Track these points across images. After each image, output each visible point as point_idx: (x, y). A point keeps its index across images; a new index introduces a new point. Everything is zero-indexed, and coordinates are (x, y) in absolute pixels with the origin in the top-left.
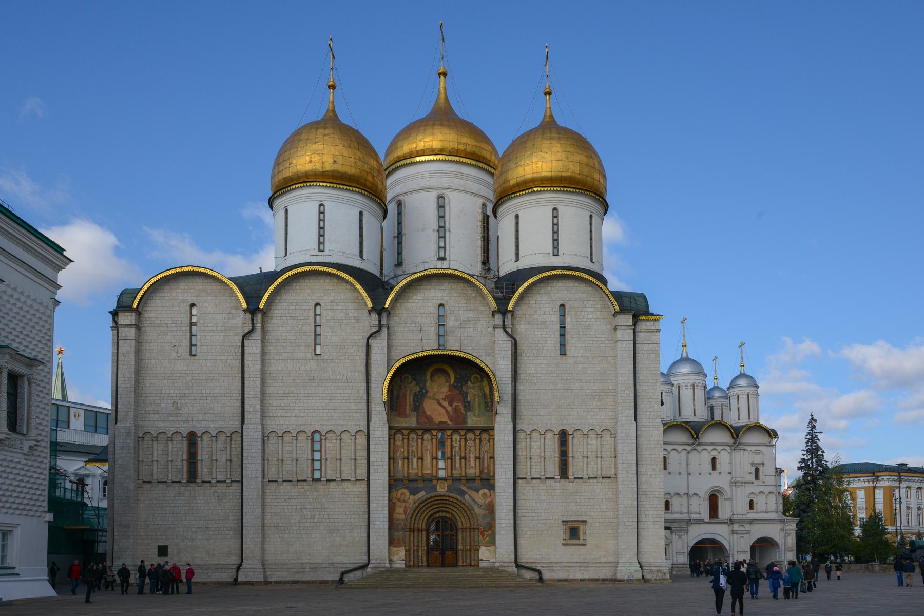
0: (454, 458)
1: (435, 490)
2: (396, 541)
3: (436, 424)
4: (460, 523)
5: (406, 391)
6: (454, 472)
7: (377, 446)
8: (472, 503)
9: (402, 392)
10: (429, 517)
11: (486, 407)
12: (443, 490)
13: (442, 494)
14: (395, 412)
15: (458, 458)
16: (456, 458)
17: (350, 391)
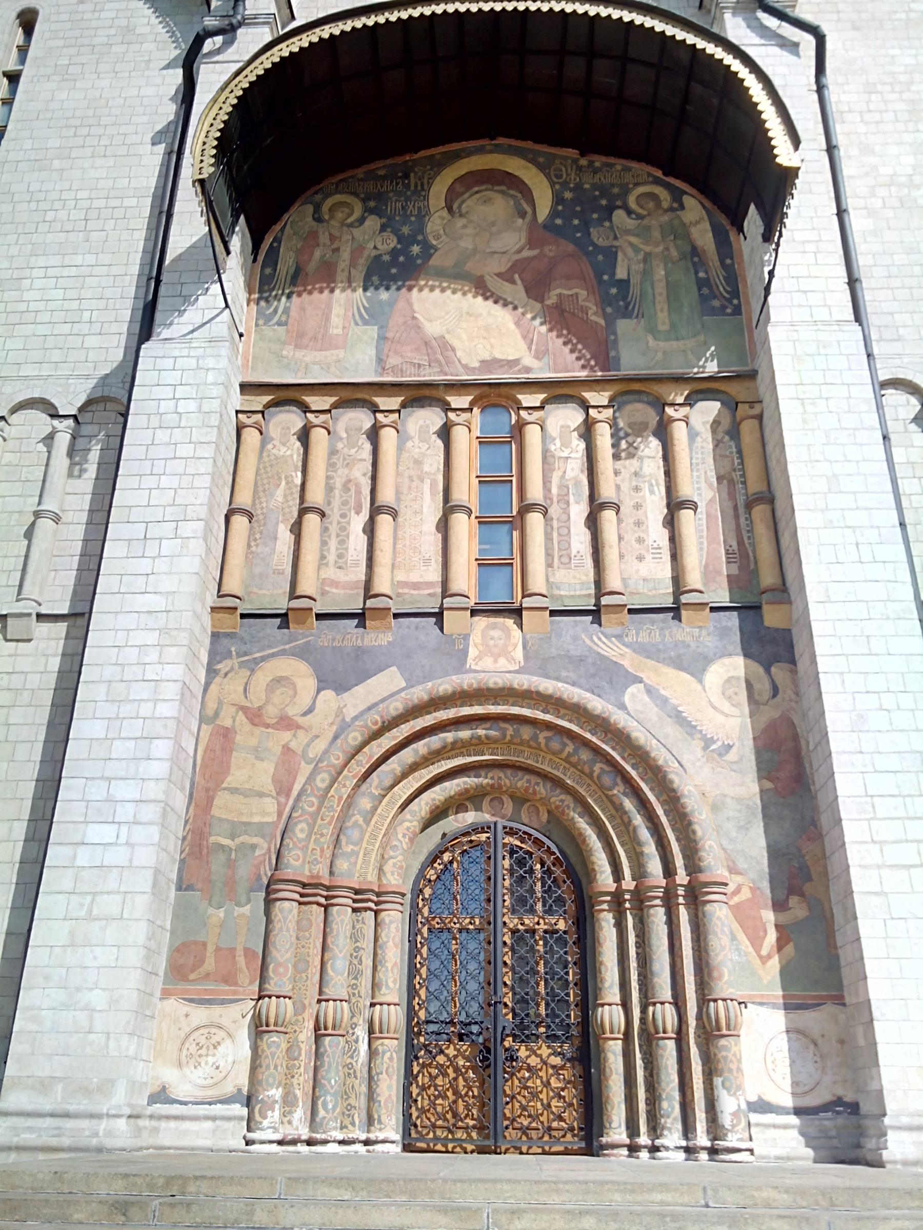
0: (554, 511)
1: (460, 665)
2: (210, 964)
3: (466, 367)
4: (601, 860)
5: (338, 249)
6: (560, 575)
7: (162, 436)
8: (671, 731)
9: (317, 253)
10: (427, 824)
11: (704, 299)
12: (503, 664)
13: (495, 681)
14: (281, 330)
15: (579, 511)
16: (566, 511)
17: (90, 259)
